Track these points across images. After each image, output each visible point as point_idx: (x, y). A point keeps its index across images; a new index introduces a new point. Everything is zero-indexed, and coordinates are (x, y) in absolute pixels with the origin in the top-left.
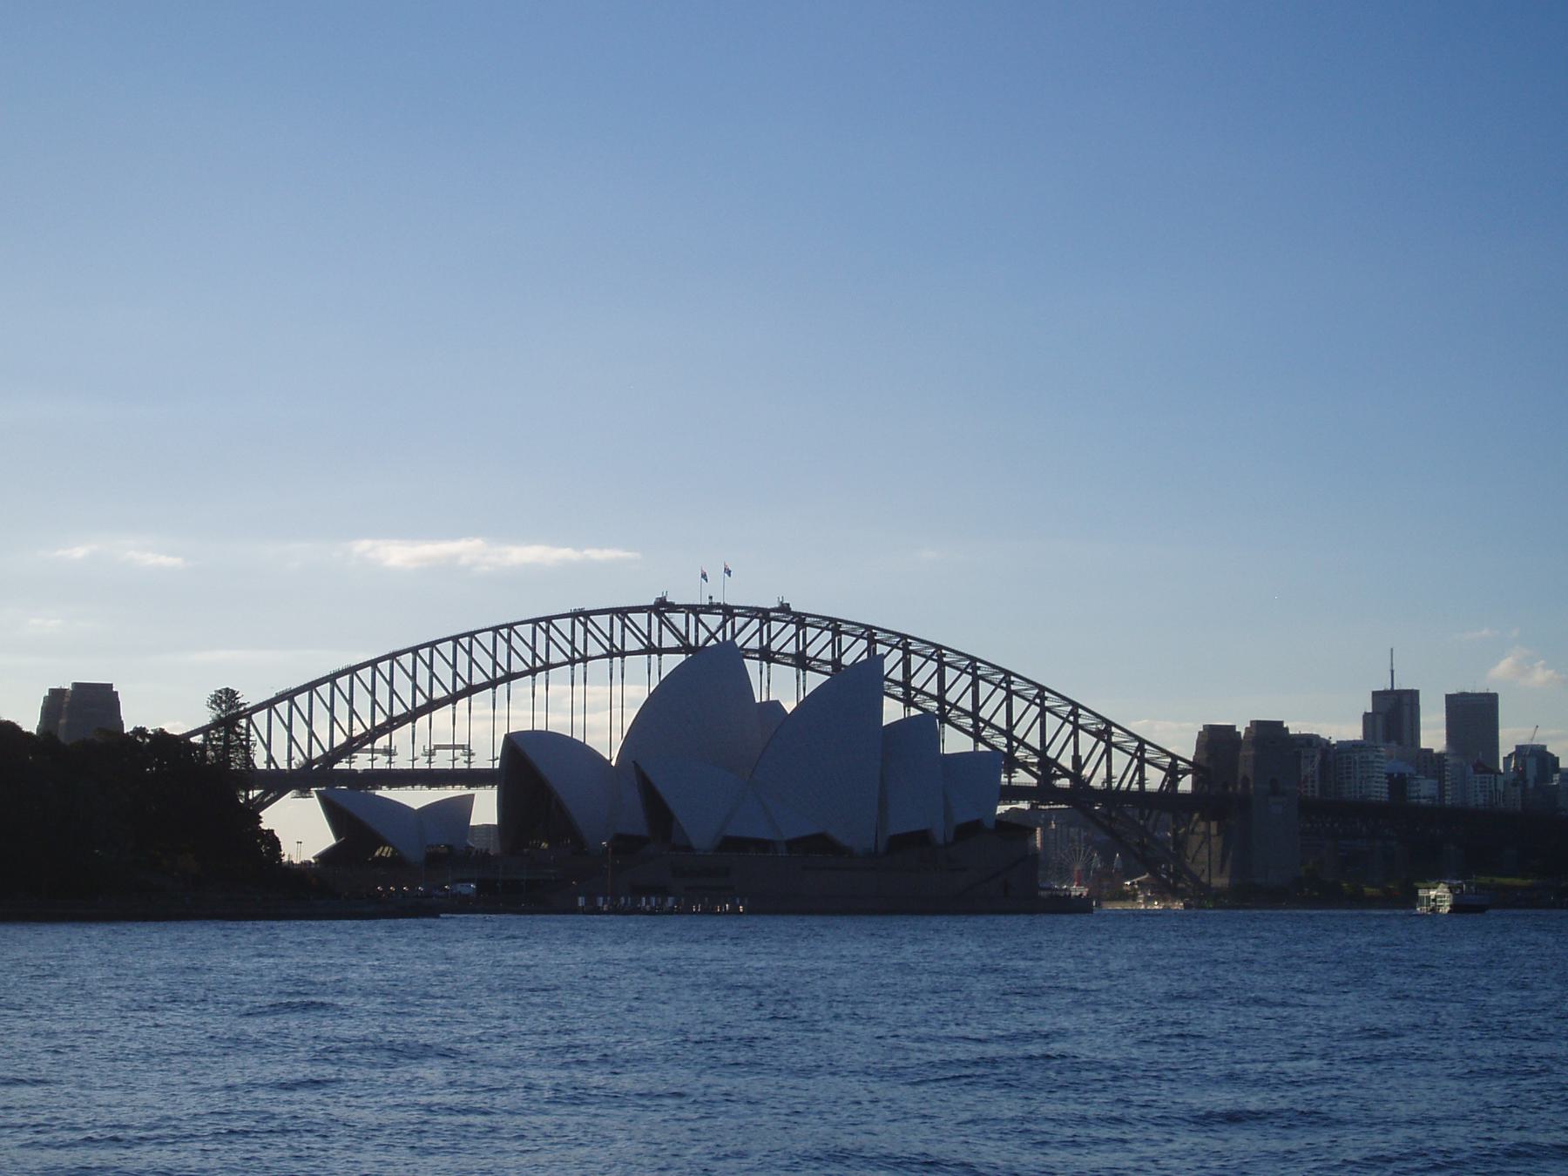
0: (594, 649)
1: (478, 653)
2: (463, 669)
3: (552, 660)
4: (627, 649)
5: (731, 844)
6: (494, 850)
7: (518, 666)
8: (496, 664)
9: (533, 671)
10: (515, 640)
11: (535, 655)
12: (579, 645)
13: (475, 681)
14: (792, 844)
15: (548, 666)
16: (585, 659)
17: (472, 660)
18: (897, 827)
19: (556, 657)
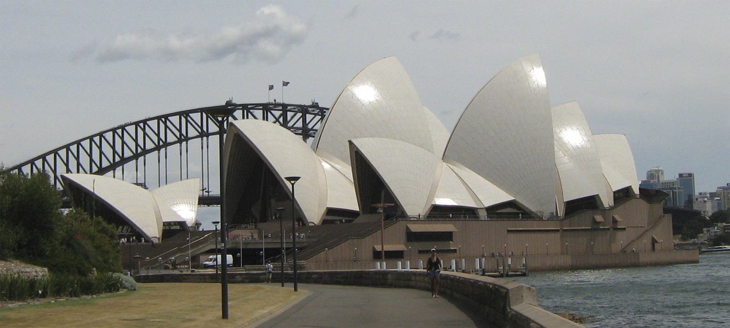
0: (192, 132)
1: (127, 138)
2: (118, 148)
3: (169, 141)
4: (210, 131)
5: (438, 212)
6: (156, 241)
7: (150, 145)
8: (137, 145)
9: (158, 148)
10: (147, 130)
11: (159, 139)
12: (184, 132)
13: (126, 156)
14: (494, 211)
15: (166, 144)
16: (187, 139)
17: (123, 143)
18: (572, 194)
19: (171, 138)
